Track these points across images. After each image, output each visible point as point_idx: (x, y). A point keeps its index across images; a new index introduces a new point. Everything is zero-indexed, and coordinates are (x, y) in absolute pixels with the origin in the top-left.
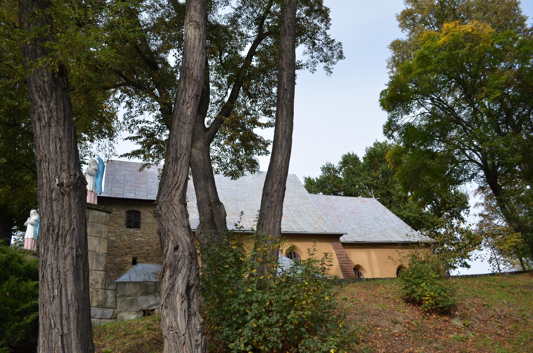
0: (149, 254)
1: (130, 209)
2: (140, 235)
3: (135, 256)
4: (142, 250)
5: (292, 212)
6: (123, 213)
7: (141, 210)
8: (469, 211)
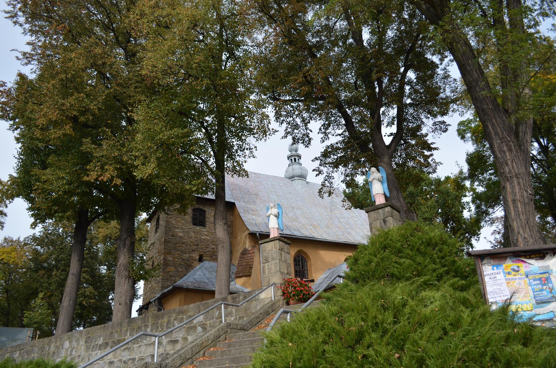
2: (206, 233)
3: (201, 253)
4: (208, 248)
5: (344, 224)
7: (206, 209)
8: (479, 238)
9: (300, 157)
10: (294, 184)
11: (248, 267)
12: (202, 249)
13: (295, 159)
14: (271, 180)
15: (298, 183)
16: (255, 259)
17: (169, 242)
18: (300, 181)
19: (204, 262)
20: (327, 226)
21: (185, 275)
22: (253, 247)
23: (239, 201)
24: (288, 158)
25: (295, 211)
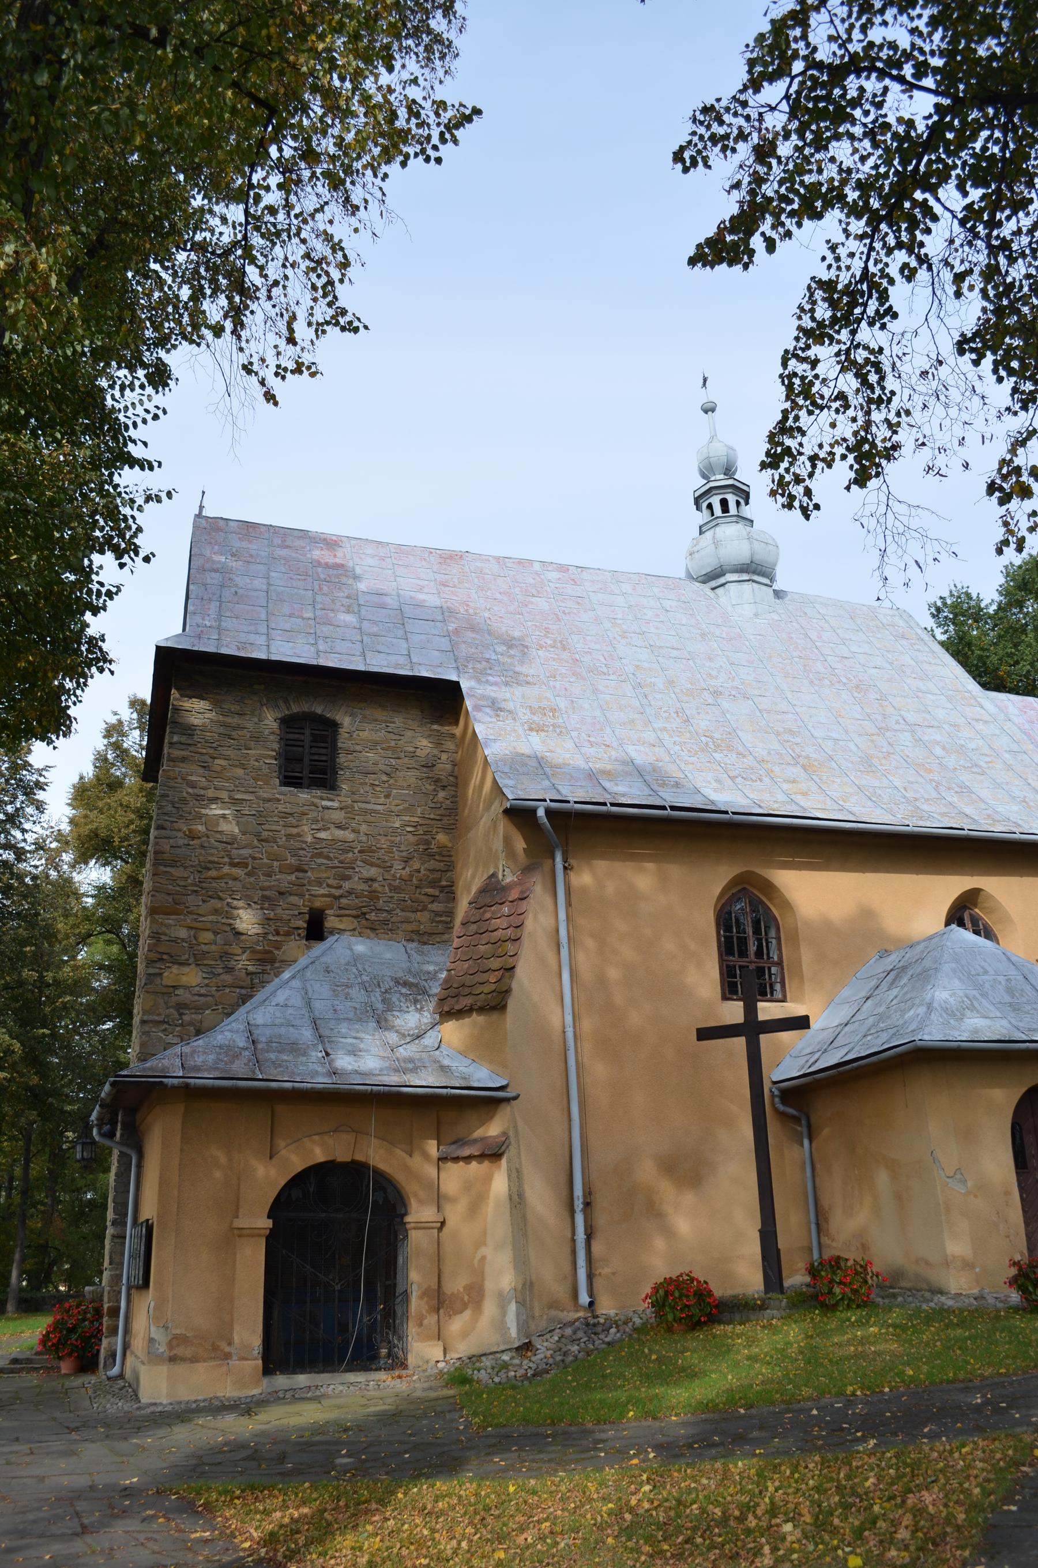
0: (373, 895)
1: (295, 709)
2: (338, 816)
3: (318, 904)
4: (348, 878)
5: (938, 751)
6: (270, 720)
7: (338, 718)
10: (723, 600)
11: (495, 963)
12: (320, 884)
13: (724, 503)
14: (627, 588)
15: (740, 597)
17: (174, 863)
18: (747, 586)
19: (331, 940)
20: (867, 764)
21: (244, 1000)
22: (527, 870)
23: (479, 676)
24: (697, 501)
25: (725, 705)
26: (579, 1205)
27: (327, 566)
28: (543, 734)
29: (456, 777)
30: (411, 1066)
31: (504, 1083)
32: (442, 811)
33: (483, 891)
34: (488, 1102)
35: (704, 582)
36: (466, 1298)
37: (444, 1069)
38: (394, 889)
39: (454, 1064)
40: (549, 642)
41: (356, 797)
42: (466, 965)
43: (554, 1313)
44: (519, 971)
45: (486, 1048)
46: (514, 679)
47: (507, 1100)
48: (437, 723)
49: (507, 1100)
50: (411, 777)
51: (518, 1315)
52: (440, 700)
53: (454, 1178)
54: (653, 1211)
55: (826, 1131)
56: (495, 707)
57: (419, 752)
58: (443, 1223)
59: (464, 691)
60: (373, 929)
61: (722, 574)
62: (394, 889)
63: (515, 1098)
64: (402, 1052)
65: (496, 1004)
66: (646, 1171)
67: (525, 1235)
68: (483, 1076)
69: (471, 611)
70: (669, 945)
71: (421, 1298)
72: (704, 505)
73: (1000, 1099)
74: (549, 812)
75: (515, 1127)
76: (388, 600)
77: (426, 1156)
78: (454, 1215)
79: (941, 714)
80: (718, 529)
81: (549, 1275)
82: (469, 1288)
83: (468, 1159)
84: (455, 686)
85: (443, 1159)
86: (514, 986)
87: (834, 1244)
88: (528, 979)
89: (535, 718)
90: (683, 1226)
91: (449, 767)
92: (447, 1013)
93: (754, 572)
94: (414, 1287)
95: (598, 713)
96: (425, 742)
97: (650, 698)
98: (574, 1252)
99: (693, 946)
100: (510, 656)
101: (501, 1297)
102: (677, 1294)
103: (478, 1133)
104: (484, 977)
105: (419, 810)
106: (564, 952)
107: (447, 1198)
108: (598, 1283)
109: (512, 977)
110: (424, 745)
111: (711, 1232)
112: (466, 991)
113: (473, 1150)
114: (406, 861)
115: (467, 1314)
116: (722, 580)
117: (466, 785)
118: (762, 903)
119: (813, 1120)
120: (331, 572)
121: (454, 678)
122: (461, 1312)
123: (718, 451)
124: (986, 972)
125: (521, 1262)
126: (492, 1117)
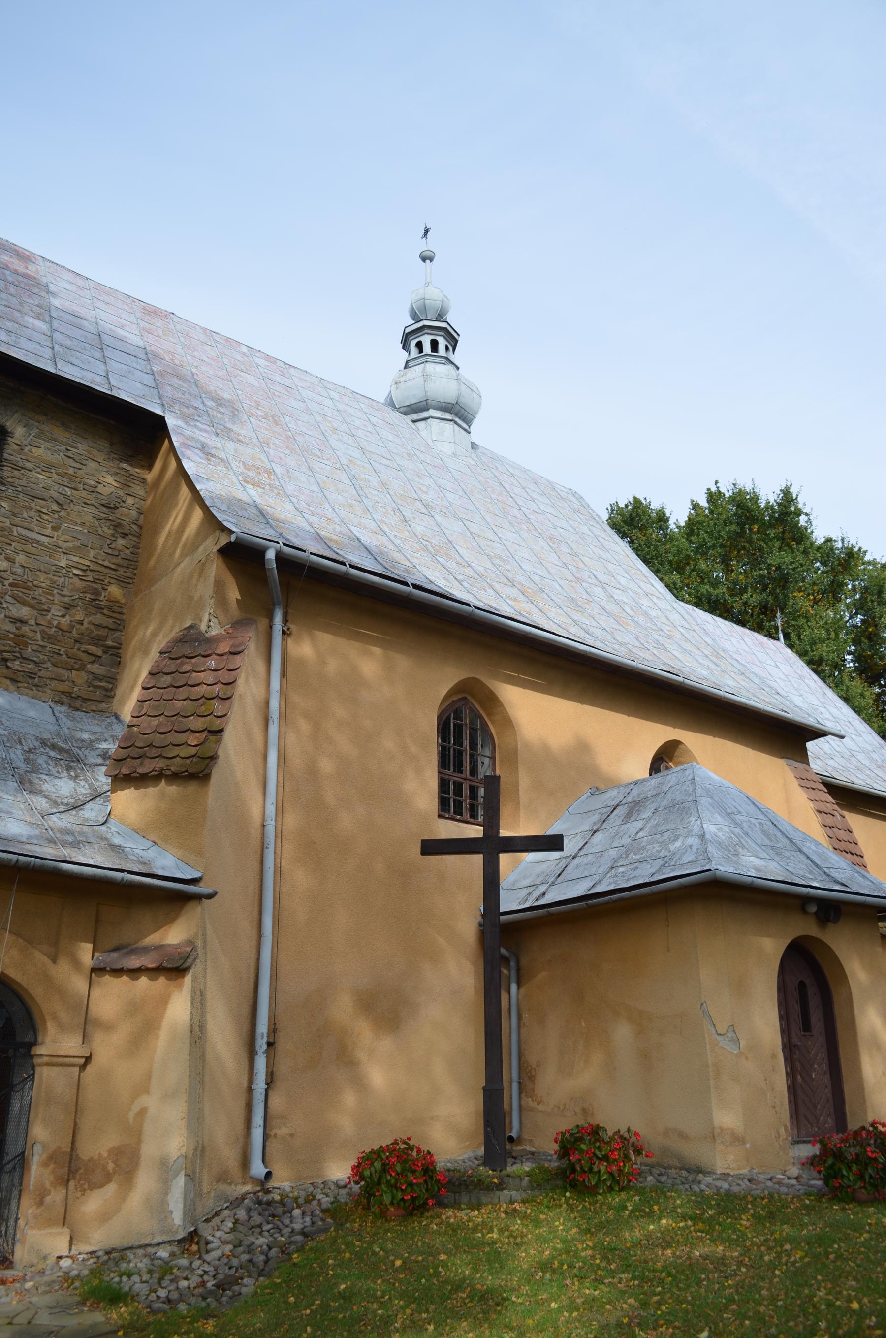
0: (20, 640)
7: (9, 425)
9: (453, 341)
11: (197, 723)
13: (434, 345)
16: (241, 682)
18: (449, 426)
22: (237, 624)
23: (186, 418)
26: (261, 1045)
27: (16, 272)
28: (260, 490)
29: (140, 527)
30: (70, 839)
31: (196, 875)
32: (119, 560)
33: (181, 640)
34: (173, 898)
35: (405, 414)
36: (111, 1166)
37: (116, 849)
38: (46, 637)
39: (128, 845)
40: (260, 413)
41: (17, 521)
42: (155, 722)
43: (222, 1187)
44: (229, 736)
45: (170, 828)
46: (227, 434)
47: (198, 897)
48: (126, 461)
49: (198, 897)
50: (88, 514)
51: (186, 1193)
52: (137, 433)
53: (111, 997)
54: (345, 1057)
55: (543, 975)
56: (206, 451)
57: (100, 488)
58: (88, 1059)
59: (170, 427)
60: (14, 681)
61: (426, 409)
62: (46, 637)
63: (210, 896)
64: (56, 821)
65: (197, 772)
66: (343, 1008)
67: (202, 1082)
68: (167, 863)
69: (177, 362)
70: (389, 744)
71: (45, 1164)
72: (413, 343)
73: (769, 947)
74: (279, 556)
75: (204, 935)
76: (86, 324)
77: (76, 964)
78: (106, 1049)
79: (623, 581)
80: (428, 365)
81: (222, 1133)
82: (117, 1153)
83: (135, 973)
84: (162, 419)
85: (98, 970)
86: (220, 753)
87: (541, 1107)
88: (234, 749)
89: (250, 474)
90: (377, 1077)
91: (134, 514)
92: (123, 780)
93: (456, 415)
94: (38, 1148)
95: (315, 488)
96: (110, 479)
97: (365, 490)
98: (249, 1108)
99: (414, 749)
100: (219, 412)
101: (165, 1169)
102: (398, 1168)
103: (153, 939)
104: (181, 738)
105: (92, 553)
106: (273, 729)
107: (99, 1024)
108: (272, 1145)
109: (219, 741)
110: (109, 484)
111: (417, 1084)
112: (154, 752)
113: (148, 961)
114: (68, 607)
115: (111, 1189)
116: (424, 415)
117: (155, 531)
118: (481, 717)
119: (524, 961)
120: (20, 278)
121: (159, 412)
122: (101, 1186)
123: (434, 296)
124: (740, 813)
125: (195, 1120)
126: (174, 919)
